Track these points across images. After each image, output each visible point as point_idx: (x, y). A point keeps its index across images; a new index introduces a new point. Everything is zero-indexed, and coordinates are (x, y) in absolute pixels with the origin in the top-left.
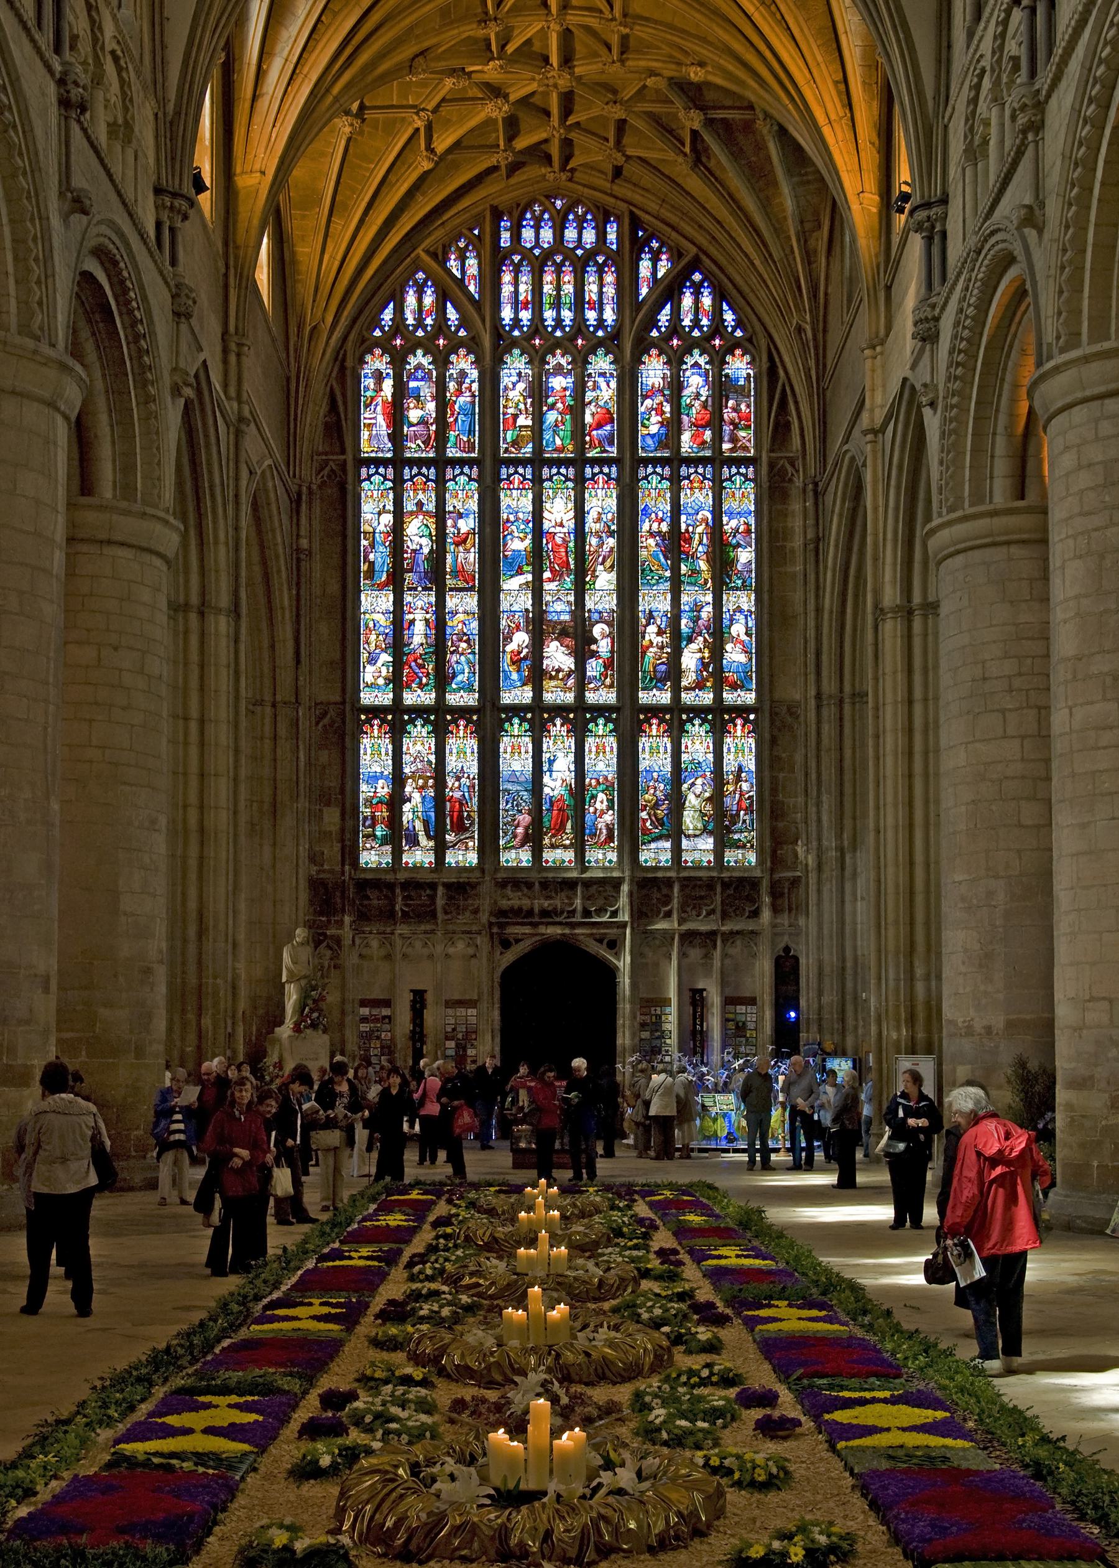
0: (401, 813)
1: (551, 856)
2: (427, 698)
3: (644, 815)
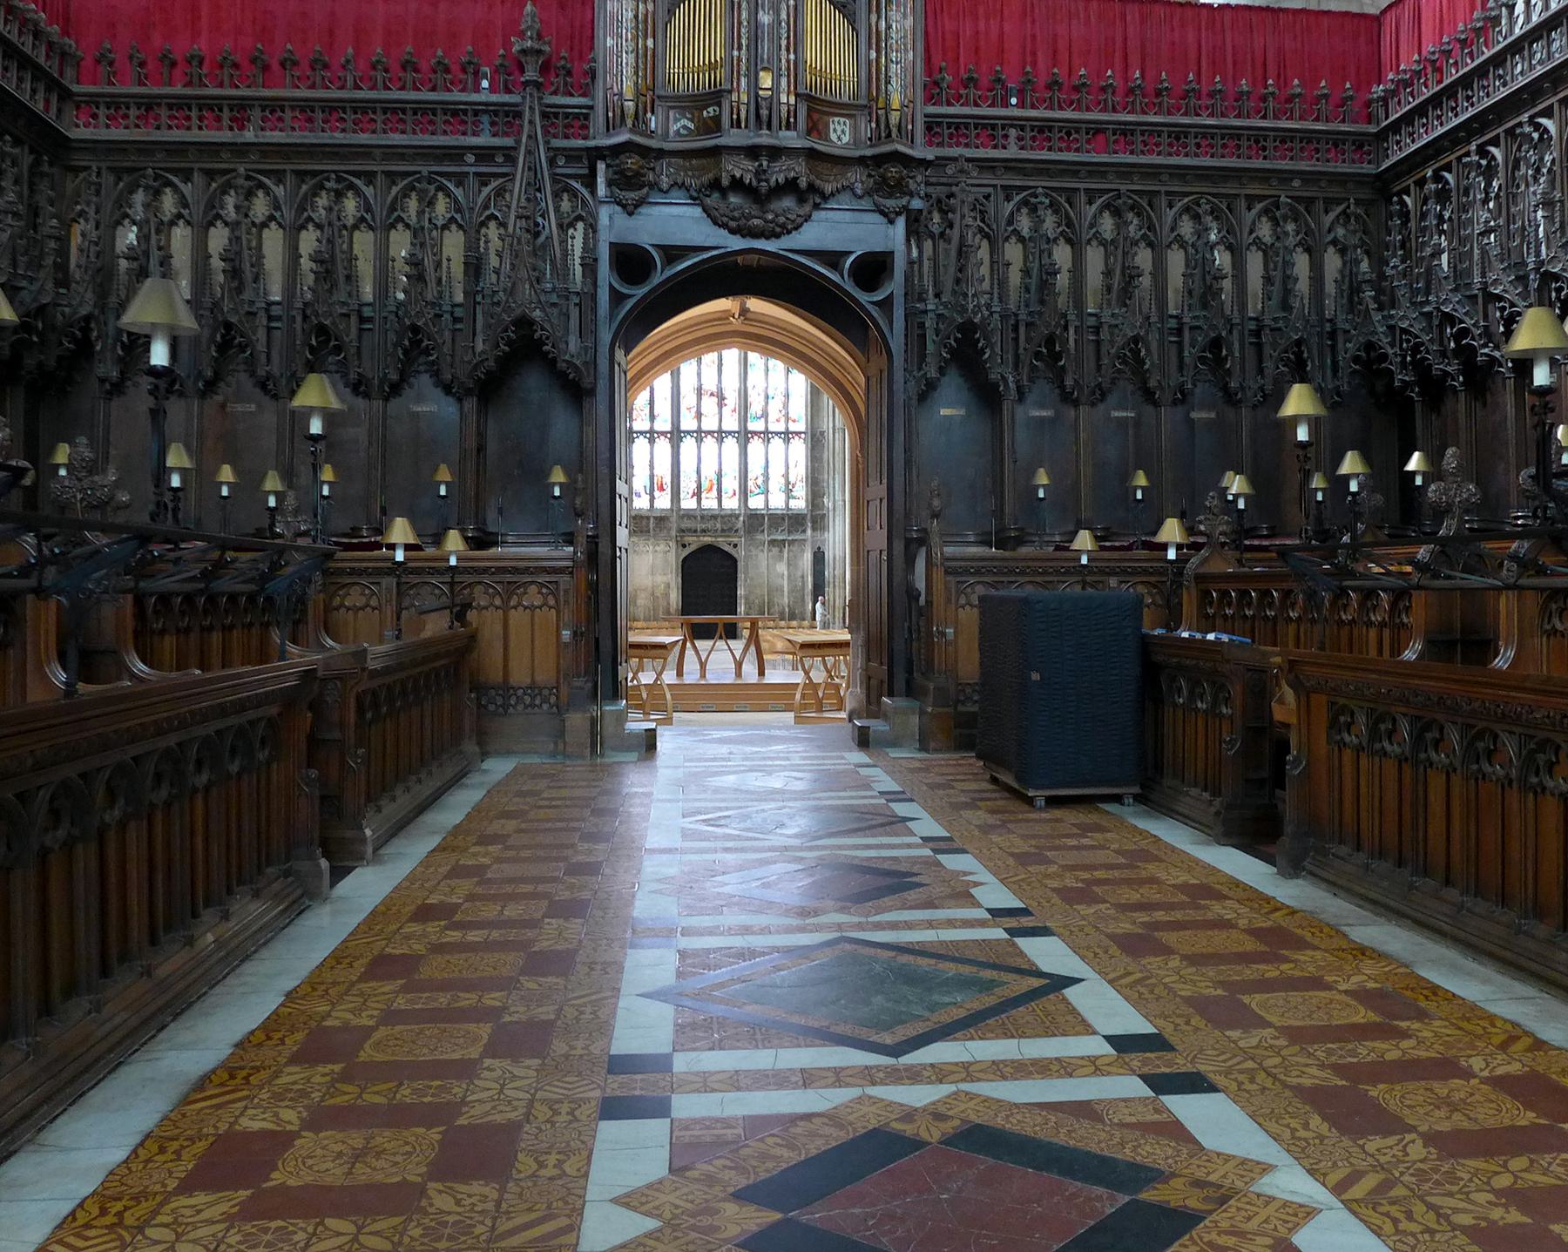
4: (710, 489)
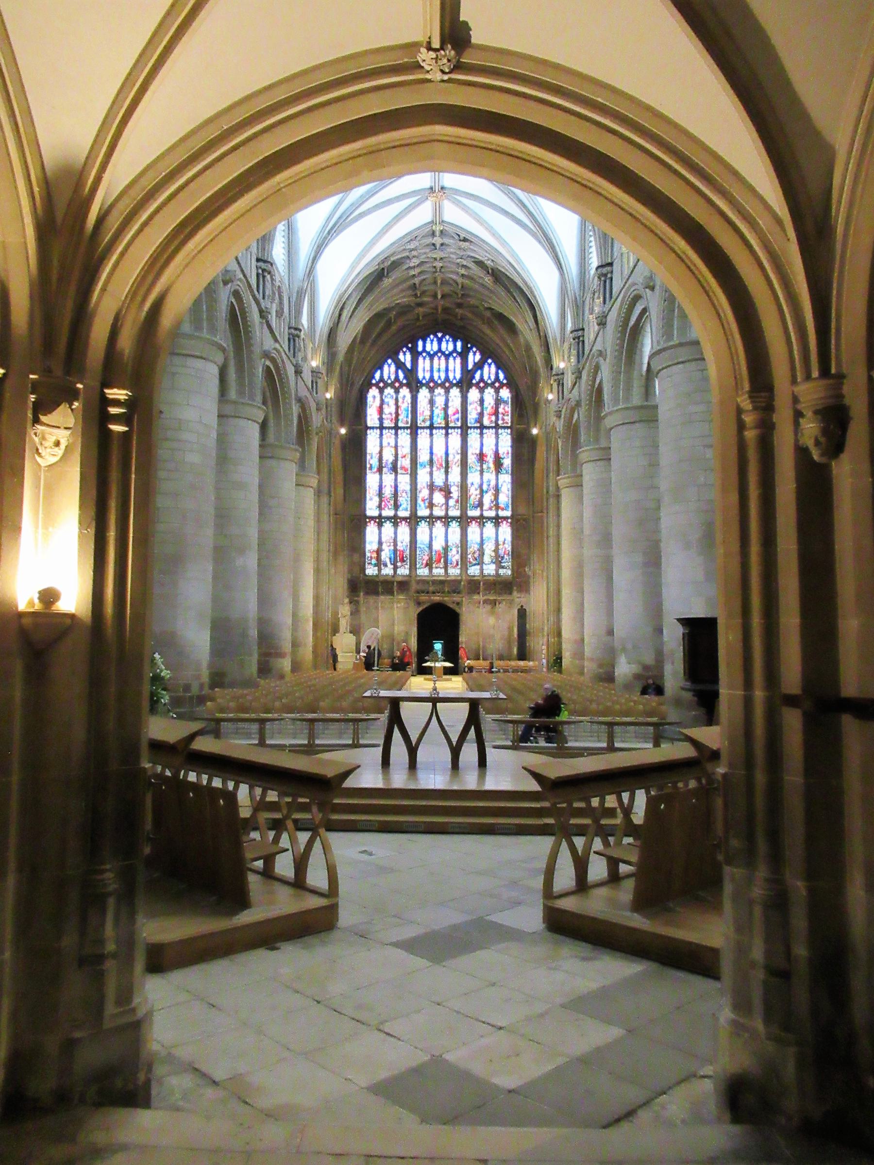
1: (435, 571)
2: (391, 513)
3: (469, 556)
4: (439, 561)
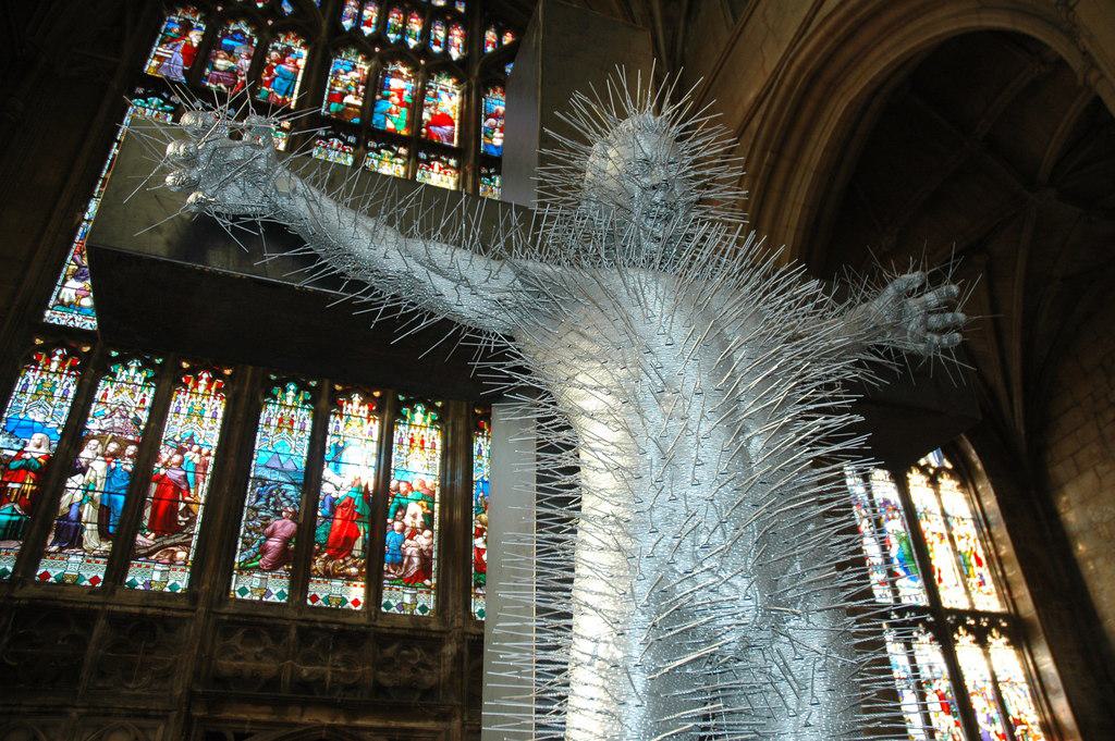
0: (61, 489)
1: (322, 591)
